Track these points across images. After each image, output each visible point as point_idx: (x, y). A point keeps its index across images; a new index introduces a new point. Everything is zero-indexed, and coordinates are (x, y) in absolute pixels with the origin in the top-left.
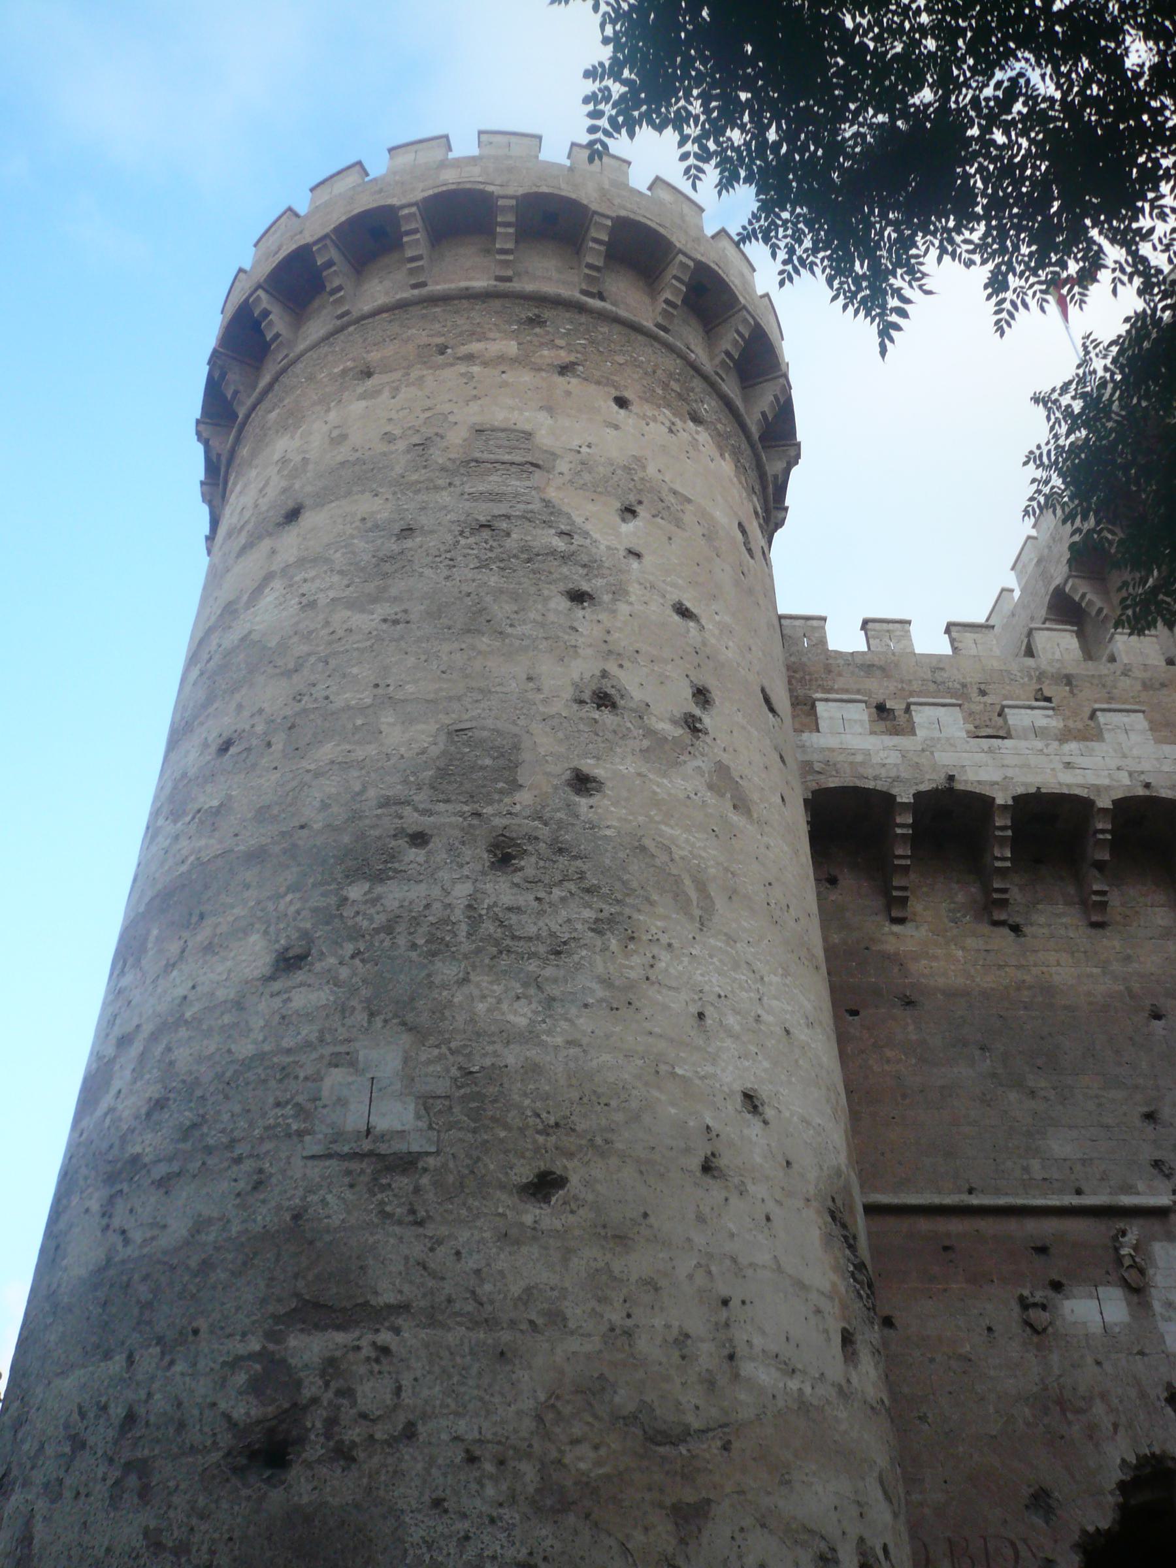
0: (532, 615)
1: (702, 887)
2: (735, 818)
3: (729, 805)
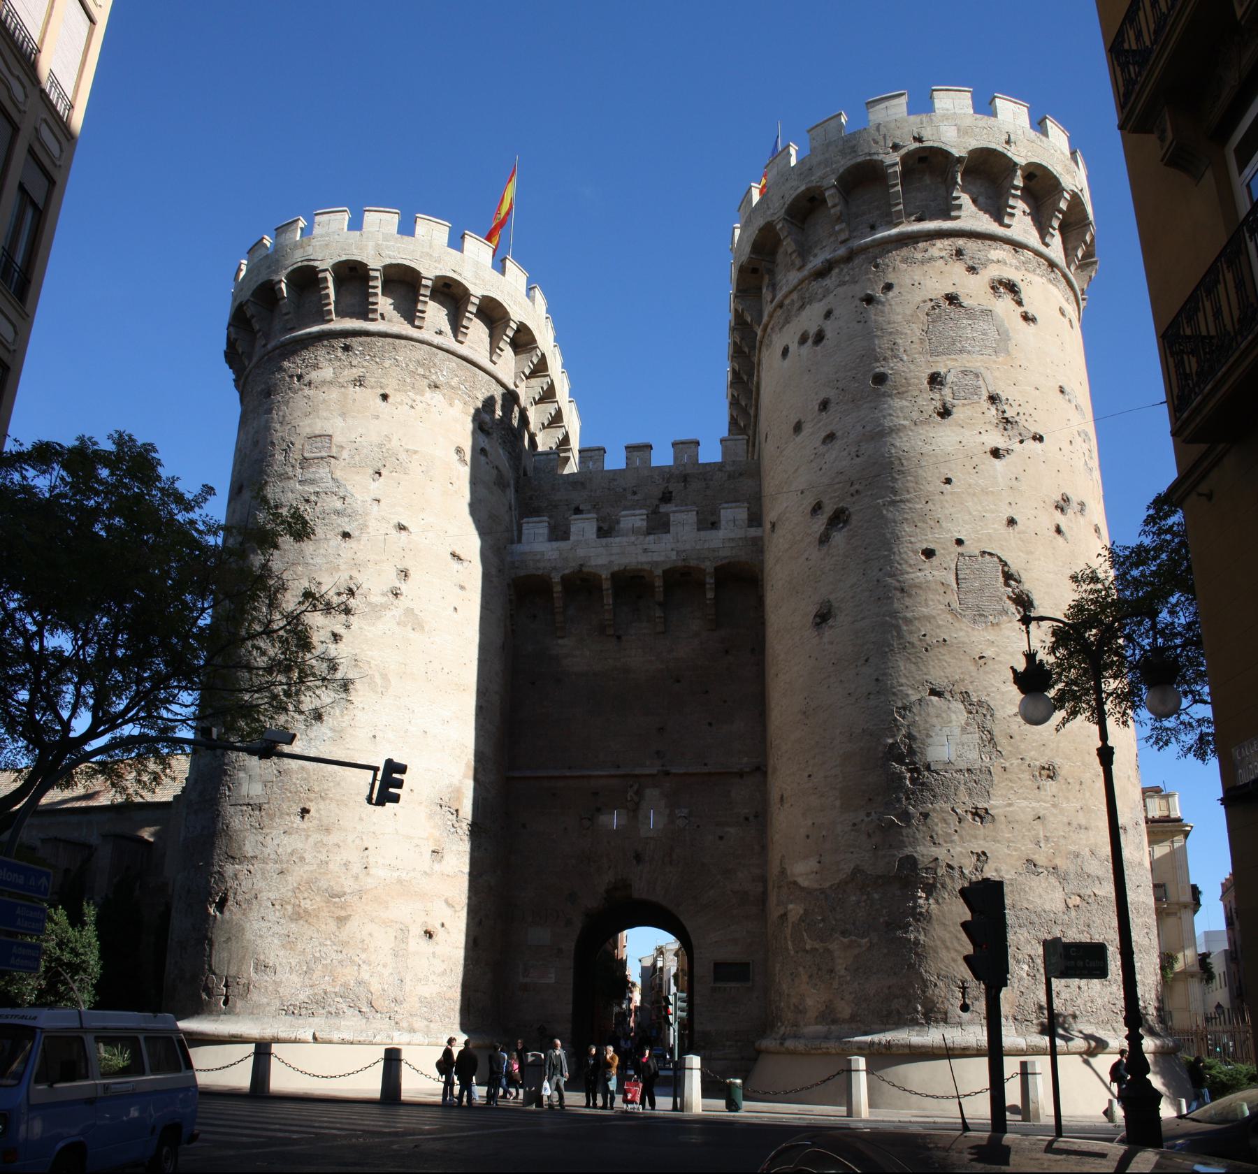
0: (322, 551)
1: (385, 677)
2: (412, 635)
3: (409, 628)
